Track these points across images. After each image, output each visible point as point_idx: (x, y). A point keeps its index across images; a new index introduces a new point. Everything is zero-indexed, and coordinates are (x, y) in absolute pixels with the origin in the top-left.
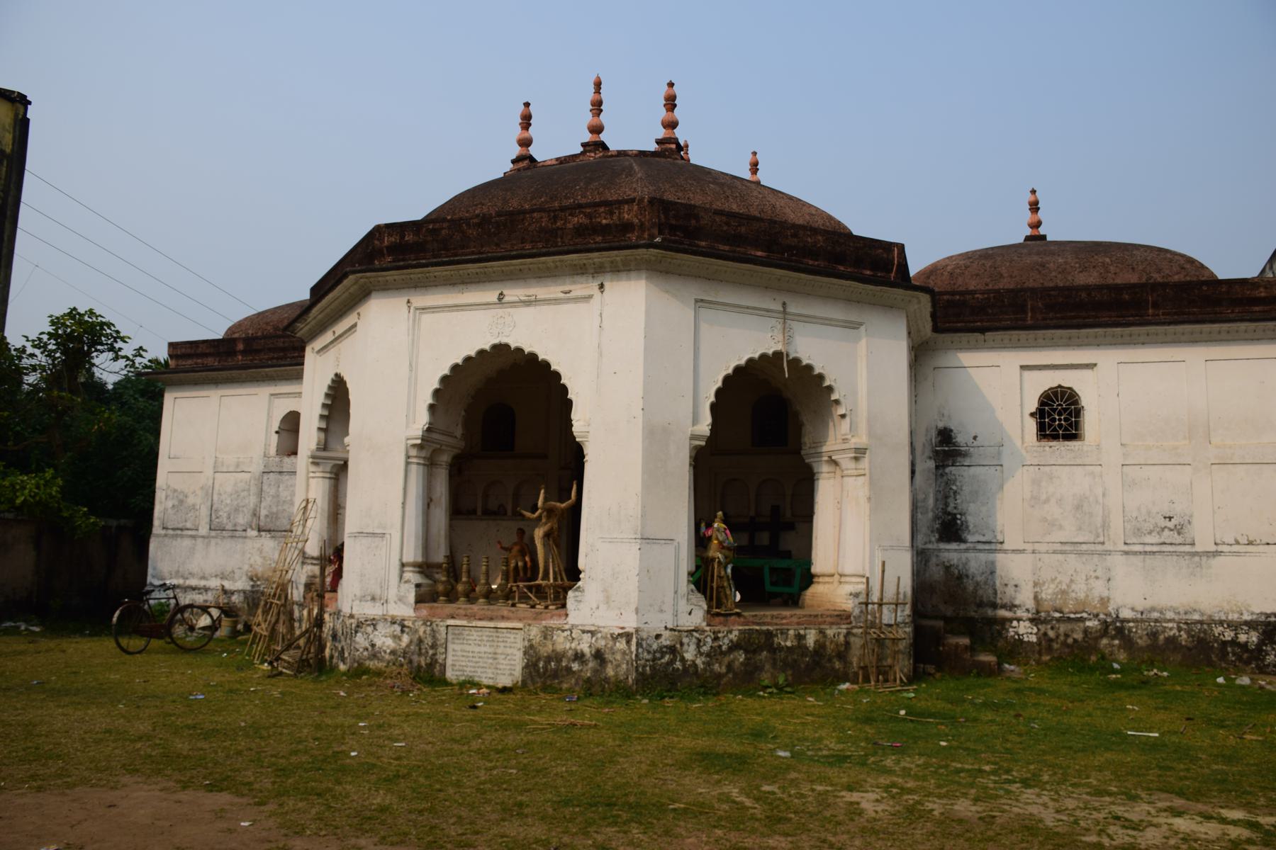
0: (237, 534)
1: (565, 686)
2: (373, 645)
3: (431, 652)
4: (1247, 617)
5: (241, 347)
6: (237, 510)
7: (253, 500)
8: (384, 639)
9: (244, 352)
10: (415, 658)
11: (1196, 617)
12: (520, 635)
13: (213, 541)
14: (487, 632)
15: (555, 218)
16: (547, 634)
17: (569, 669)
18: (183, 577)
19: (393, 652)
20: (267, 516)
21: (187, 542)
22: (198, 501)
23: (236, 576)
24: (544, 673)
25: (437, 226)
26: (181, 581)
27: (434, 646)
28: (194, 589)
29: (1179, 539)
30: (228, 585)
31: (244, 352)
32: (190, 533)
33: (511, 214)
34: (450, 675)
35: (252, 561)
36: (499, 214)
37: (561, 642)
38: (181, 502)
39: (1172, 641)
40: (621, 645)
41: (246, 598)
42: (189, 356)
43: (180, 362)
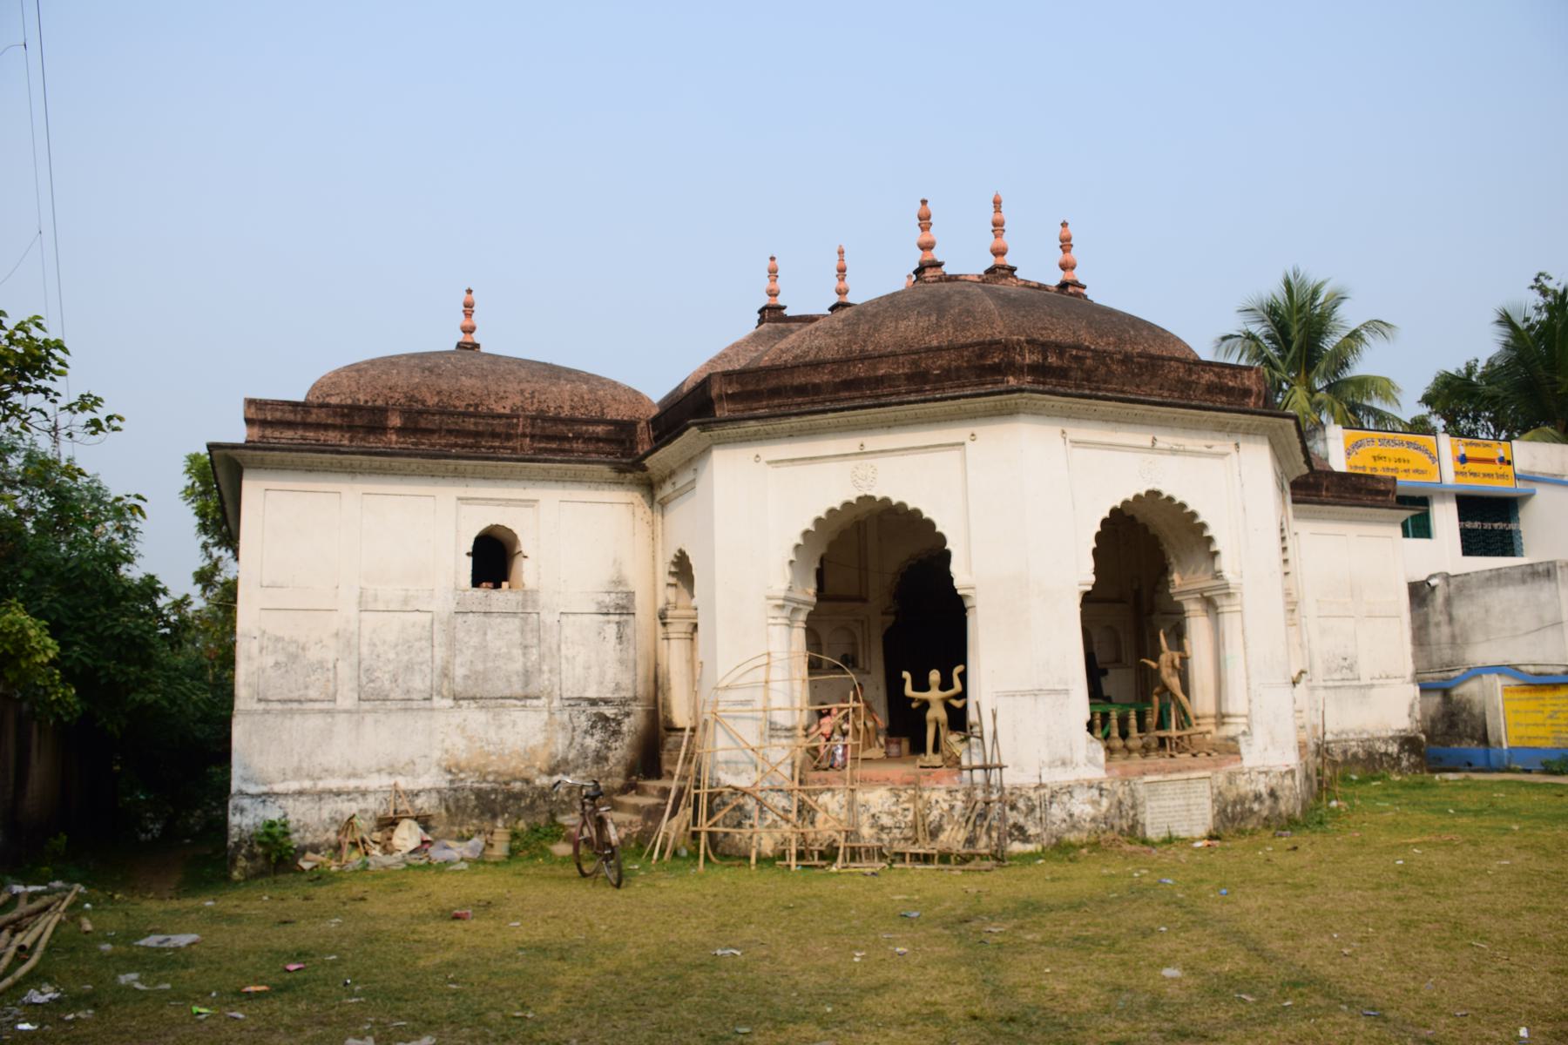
0: (415, 705)
1: (1250, 827)
2: (1071, 816)
3: (1131, 813)
4: (1390, 734)
5: (395, 421)
6: (409, 668)
7: (440, 653)
8: (1082, 807)
9: (400, 431)
10: (1117, 822)
11: (1365, 736)
12: (1207, 783)
13: (369, 718)
14: (1179, 785)
15: (1190, 371)
16: (1231, 778)
17: (1251, 810)
18: (309, 776)
19: (1093, 820)
20: (466, 677)
21: (315, 722)
22: (330, 656)
23: (419, 769)
24: (1233, 819)
25: (1081, 353)
26: (307, 784)
27: (1133, 807)
28: (338, 794)
29: (1350, 676)
30: (404, 783)
31: (400, 431)
32: (318, 706)
33: (1152, 357)
34: (1151, 834)
35: (447, 744)
36: (1140, 355)
37: (1244, 786)
38: (294, 658)
39: (1355, 755)
40: (1288, 781)
41: (442, 799)
42: (290, 425)
43: (268, 432)
